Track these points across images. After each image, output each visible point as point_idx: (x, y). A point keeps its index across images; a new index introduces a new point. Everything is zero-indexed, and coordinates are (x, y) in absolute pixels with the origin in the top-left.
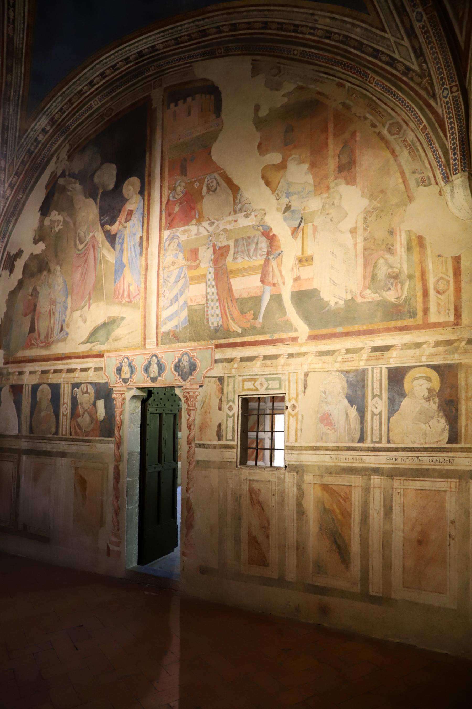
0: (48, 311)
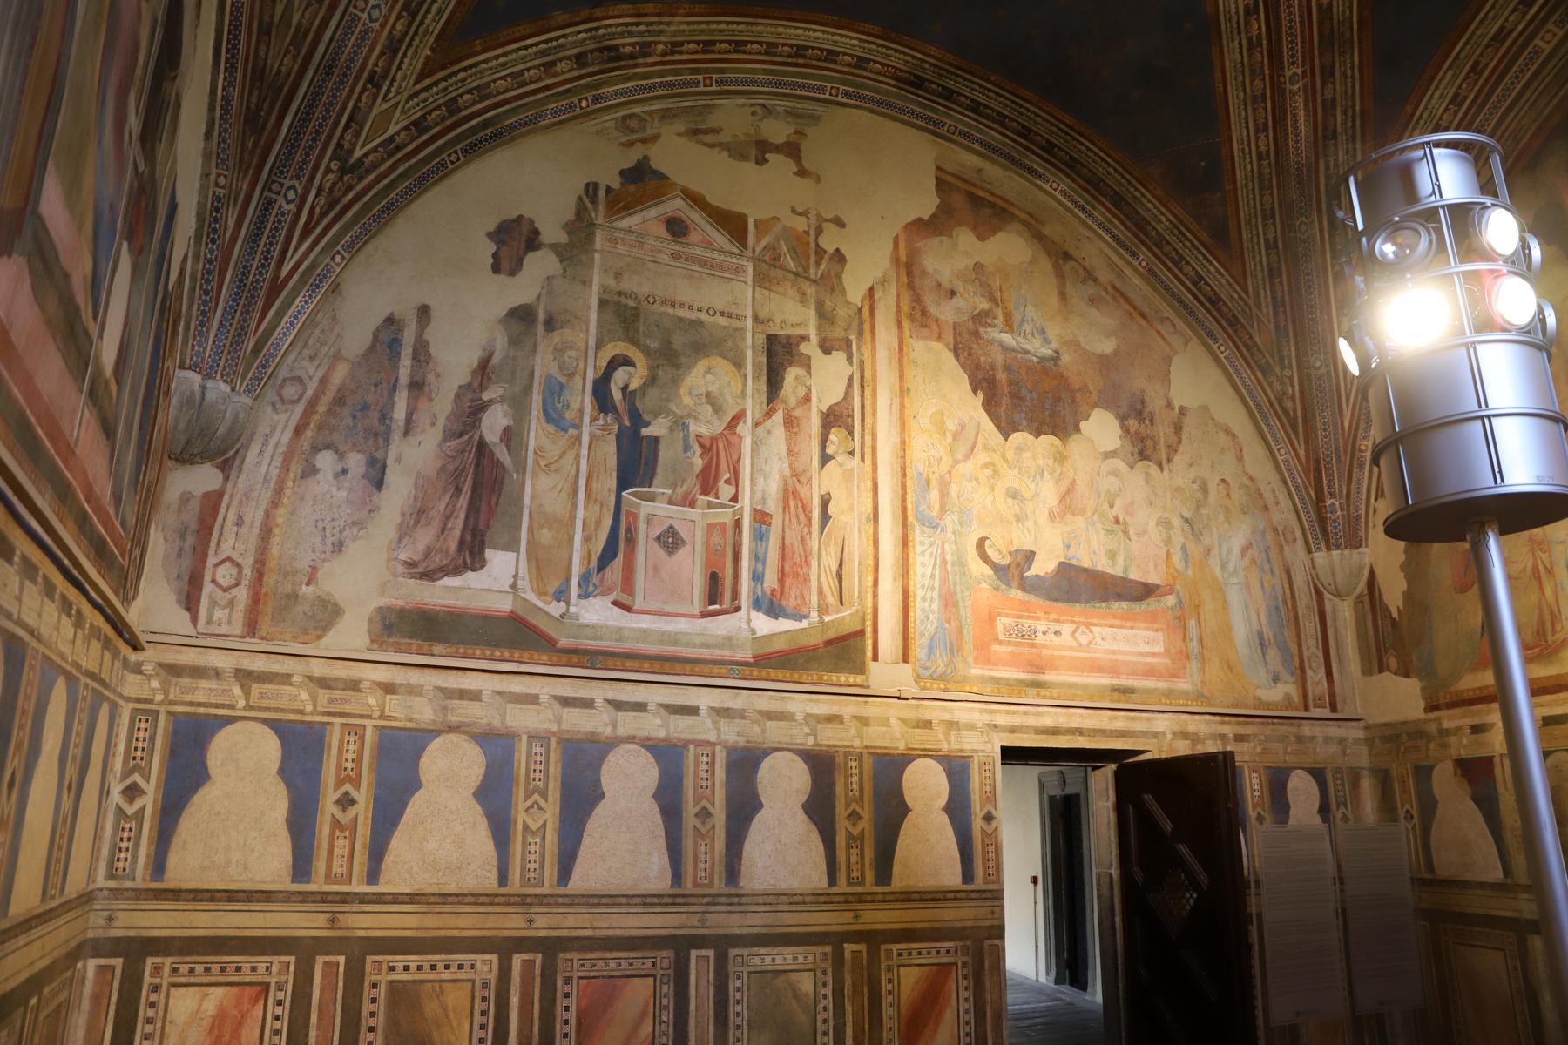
0: (1529, 570)
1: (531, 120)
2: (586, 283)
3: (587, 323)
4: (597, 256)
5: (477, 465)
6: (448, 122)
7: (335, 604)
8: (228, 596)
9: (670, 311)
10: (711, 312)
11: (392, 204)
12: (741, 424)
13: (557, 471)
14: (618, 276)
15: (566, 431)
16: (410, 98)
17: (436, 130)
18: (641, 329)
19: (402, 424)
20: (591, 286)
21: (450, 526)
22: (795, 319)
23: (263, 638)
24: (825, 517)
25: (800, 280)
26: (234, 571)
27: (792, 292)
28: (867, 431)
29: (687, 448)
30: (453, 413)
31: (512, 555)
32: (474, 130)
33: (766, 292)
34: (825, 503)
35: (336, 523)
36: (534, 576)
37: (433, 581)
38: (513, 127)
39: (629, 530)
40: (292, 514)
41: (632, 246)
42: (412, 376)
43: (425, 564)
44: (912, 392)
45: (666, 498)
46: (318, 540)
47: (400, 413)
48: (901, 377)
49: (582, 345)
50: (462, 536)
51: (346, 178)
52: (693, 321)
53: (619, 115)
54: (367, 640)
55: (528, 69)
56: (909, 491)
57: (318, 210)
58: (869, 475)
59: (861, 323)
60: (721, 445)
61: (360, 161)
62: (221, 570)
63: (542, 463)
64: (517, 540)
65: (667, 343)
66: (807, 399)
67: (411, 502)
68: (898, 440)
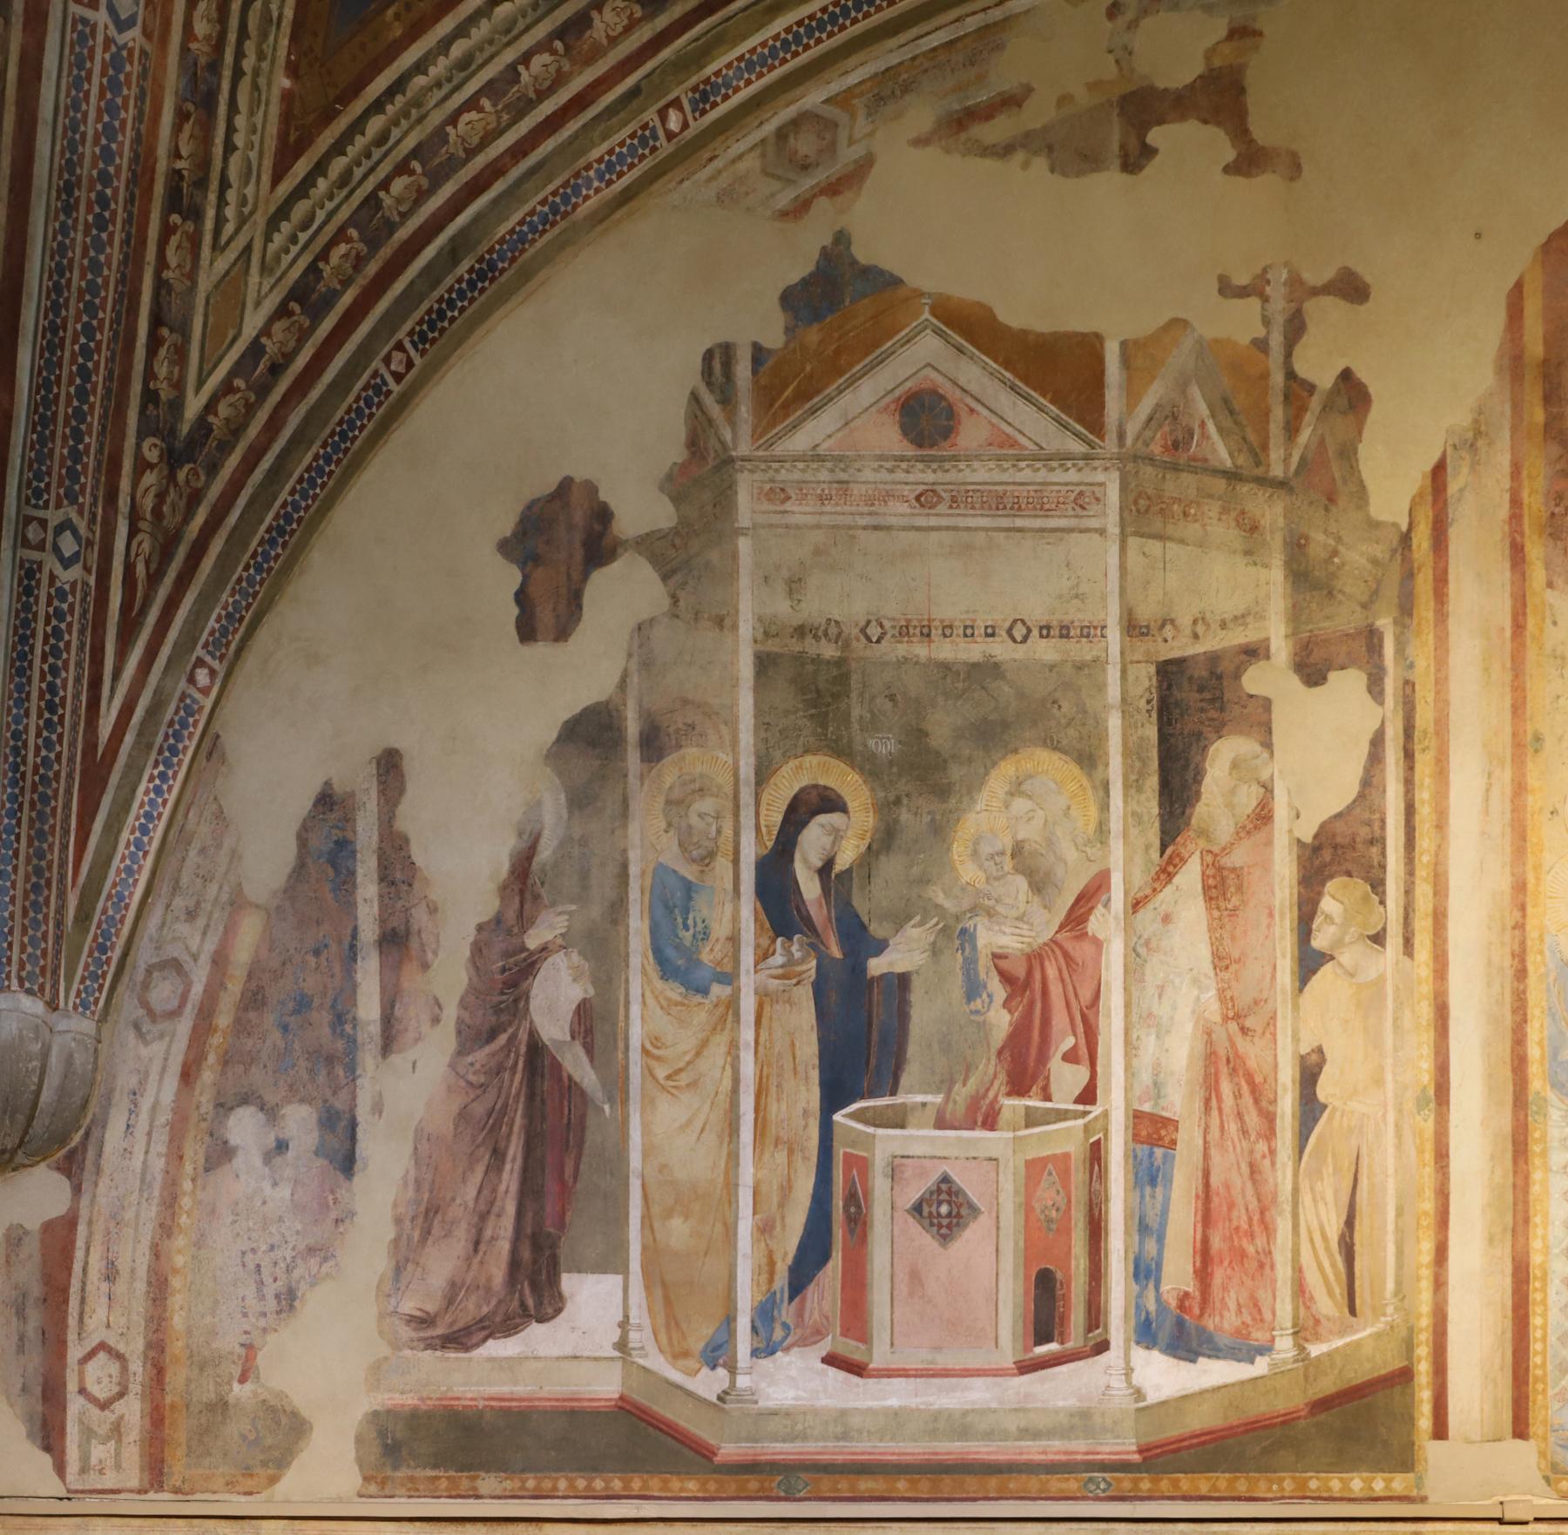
1: (555, 210)
2: (723, 622)
3: (733, 723)
4: (744, 545)
5: (531, 1097)
6: (372, 269)
7: (294, 1414)
8: (108, 1416)
9: (921, 651)
10: (1019, 632)
11: (288, 518)
12: (1099, 909)
13: (693, 1085)
14: (794, 586)
15: (705, 991)
16: (273, 225)
17: (347, 299)
18: (856, 712)
19: (375, 1029)
20: (735, 627)
21: (488, 1233)
22: (1228, 606)
23: (176, 1491)
24: (1310, 1109)
25: (1244, 489)
26: (114, 1368)
27: (1223, 531)
28: (1421, 873)
29: (973, 989)
30: (472, 990)
31: (617, 1280)
32: (432, 274)
33: (1155, 547)
34: (1309, 1074)
35: (278, 1254)
37: (467, 1349)
38: (518, 240)
39: (851, 1198)
41: (822, 499)
42: (382, 921)
43: (448, 1318)
44: (1549, 744)
45: (930, 1115)
46: (250, 1292)
47: (369, 1008)
48: (1518, 709)
49: (724, 780)
50: (514, 1251)
51: (181, 475)
52: (975, 665)
53: (770, 128)
54: (359, 1481)
55: (526, 59)
56: (1534, 1011)
57: (140, 569)
58: (1426, 989)
59: (1409, 575)
60: (1052, 972)
61: (202, 425)
62: (91, 1367)
63: (661, 1073)
64: (623, 1246)
65: (917, 735)
66: (1263, 816)
67: (410, 1193)
68: (1505, 884)
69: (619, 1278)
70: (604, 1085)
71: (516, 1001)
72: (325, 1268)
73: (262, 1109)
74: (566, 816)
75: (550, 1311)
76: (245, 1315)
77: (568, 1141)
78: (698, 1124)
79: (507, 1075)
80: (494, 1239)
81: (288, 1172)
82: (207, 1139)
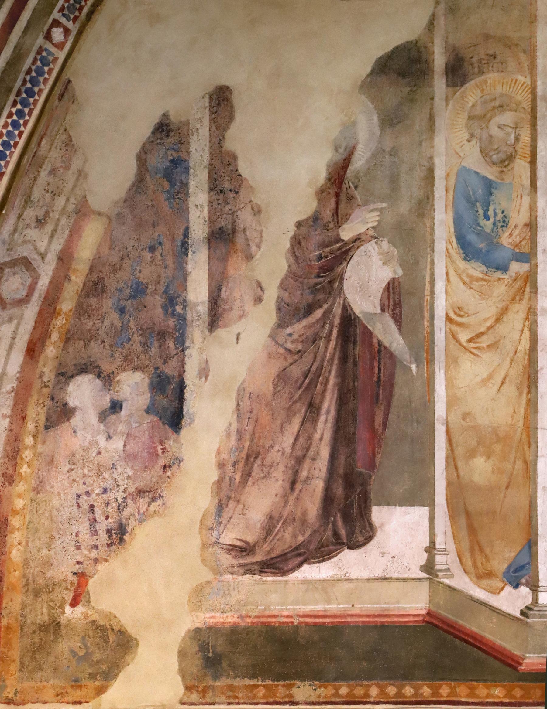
5: (344, 360)
7: (122, 632)
13: (492, 346)
19: (203, 309)
21: (304, 474)
35: (110, 496)
36: (466, 544)
37: (284, 573)
40: (37, 490)
43: (266, 547)
46: (84, 528)
63: (463, 337)
64: (430, 482)
69: (425, 510)
70: (411, 348)
71: (331, 282)
72: (154, 506)
73: (99, 376)
74: (378, 133)
75: (361, 539)
76: (78, 548)
77: (378, 394)
78: (498, 379)
79: (322, 343)
80: (309, 478)
81: (121, 428)
82: (48, 402)
